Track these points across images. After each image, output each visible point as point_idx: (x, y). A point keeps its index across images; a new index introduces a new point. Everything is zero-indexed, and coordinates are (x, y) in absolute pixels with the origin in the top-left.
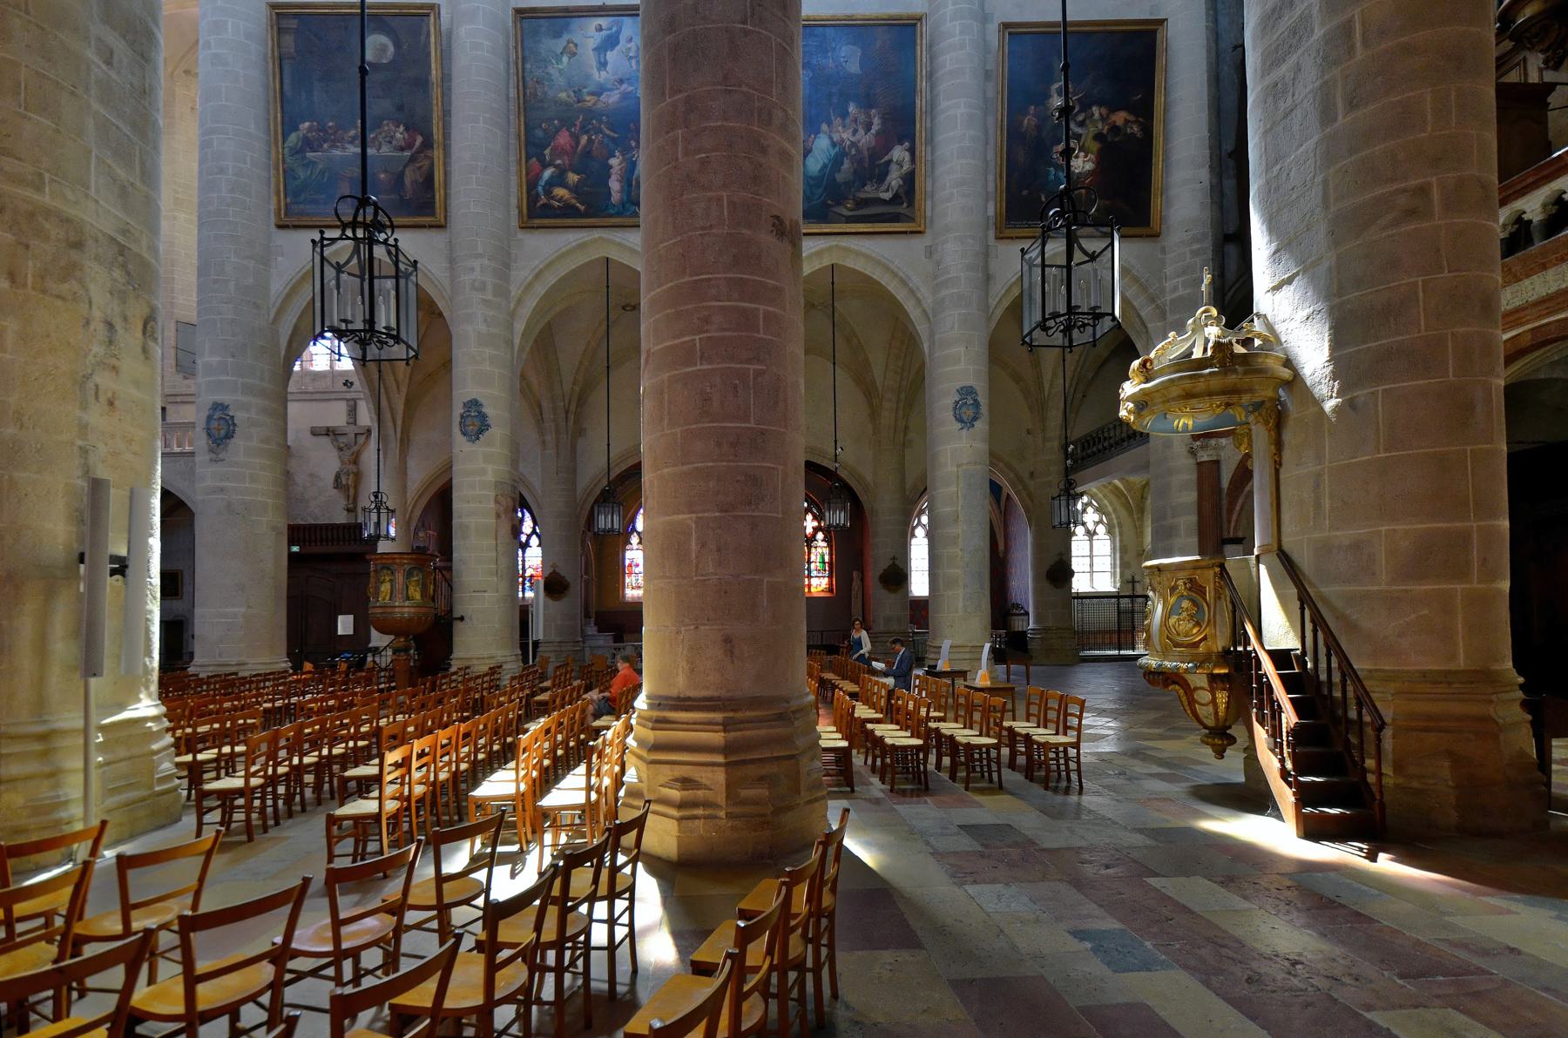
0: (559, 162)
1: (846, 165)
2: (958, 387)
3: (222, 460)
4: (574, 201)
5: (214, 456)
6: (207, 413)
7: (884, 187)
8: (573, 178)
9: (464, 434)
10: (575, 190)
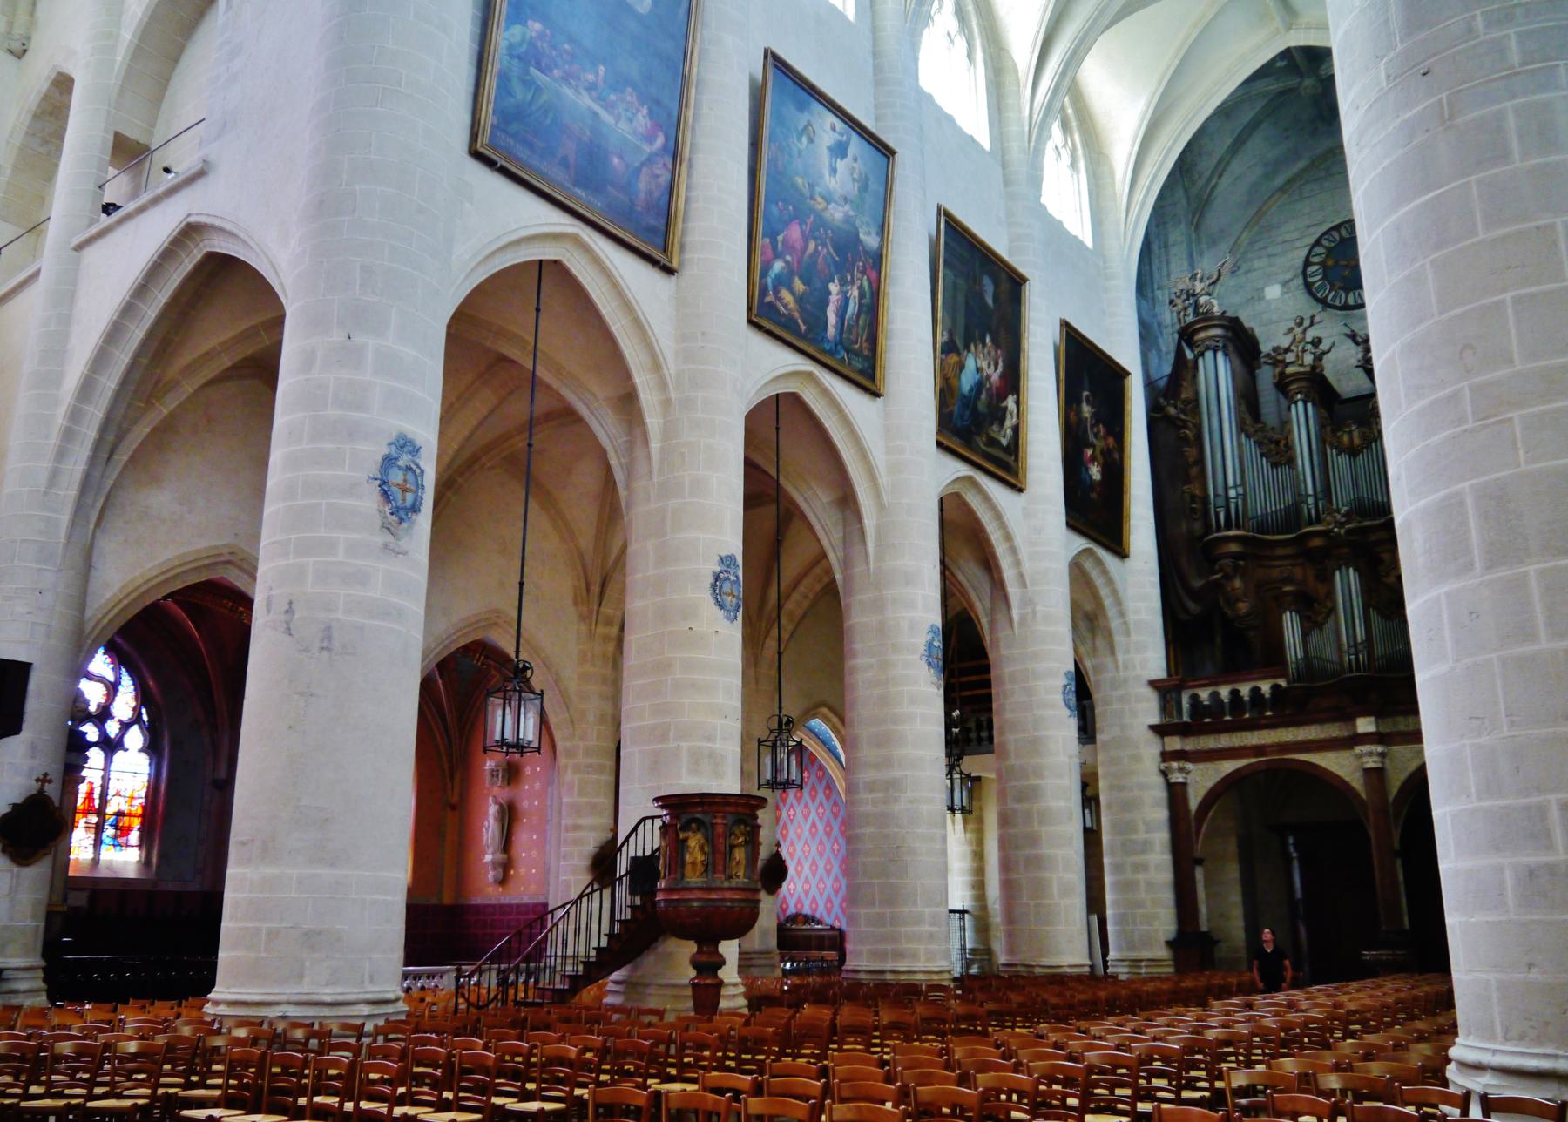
0: (788, 258)
1: (983, 396)
2: (1065, 670)
3: (405, 553)
4: (797, 315)
5: (390, 538)
6: (385, 450)
7: (1003, 433)
8: (799, 286)
9: (721, 605)
10: (800, 300)
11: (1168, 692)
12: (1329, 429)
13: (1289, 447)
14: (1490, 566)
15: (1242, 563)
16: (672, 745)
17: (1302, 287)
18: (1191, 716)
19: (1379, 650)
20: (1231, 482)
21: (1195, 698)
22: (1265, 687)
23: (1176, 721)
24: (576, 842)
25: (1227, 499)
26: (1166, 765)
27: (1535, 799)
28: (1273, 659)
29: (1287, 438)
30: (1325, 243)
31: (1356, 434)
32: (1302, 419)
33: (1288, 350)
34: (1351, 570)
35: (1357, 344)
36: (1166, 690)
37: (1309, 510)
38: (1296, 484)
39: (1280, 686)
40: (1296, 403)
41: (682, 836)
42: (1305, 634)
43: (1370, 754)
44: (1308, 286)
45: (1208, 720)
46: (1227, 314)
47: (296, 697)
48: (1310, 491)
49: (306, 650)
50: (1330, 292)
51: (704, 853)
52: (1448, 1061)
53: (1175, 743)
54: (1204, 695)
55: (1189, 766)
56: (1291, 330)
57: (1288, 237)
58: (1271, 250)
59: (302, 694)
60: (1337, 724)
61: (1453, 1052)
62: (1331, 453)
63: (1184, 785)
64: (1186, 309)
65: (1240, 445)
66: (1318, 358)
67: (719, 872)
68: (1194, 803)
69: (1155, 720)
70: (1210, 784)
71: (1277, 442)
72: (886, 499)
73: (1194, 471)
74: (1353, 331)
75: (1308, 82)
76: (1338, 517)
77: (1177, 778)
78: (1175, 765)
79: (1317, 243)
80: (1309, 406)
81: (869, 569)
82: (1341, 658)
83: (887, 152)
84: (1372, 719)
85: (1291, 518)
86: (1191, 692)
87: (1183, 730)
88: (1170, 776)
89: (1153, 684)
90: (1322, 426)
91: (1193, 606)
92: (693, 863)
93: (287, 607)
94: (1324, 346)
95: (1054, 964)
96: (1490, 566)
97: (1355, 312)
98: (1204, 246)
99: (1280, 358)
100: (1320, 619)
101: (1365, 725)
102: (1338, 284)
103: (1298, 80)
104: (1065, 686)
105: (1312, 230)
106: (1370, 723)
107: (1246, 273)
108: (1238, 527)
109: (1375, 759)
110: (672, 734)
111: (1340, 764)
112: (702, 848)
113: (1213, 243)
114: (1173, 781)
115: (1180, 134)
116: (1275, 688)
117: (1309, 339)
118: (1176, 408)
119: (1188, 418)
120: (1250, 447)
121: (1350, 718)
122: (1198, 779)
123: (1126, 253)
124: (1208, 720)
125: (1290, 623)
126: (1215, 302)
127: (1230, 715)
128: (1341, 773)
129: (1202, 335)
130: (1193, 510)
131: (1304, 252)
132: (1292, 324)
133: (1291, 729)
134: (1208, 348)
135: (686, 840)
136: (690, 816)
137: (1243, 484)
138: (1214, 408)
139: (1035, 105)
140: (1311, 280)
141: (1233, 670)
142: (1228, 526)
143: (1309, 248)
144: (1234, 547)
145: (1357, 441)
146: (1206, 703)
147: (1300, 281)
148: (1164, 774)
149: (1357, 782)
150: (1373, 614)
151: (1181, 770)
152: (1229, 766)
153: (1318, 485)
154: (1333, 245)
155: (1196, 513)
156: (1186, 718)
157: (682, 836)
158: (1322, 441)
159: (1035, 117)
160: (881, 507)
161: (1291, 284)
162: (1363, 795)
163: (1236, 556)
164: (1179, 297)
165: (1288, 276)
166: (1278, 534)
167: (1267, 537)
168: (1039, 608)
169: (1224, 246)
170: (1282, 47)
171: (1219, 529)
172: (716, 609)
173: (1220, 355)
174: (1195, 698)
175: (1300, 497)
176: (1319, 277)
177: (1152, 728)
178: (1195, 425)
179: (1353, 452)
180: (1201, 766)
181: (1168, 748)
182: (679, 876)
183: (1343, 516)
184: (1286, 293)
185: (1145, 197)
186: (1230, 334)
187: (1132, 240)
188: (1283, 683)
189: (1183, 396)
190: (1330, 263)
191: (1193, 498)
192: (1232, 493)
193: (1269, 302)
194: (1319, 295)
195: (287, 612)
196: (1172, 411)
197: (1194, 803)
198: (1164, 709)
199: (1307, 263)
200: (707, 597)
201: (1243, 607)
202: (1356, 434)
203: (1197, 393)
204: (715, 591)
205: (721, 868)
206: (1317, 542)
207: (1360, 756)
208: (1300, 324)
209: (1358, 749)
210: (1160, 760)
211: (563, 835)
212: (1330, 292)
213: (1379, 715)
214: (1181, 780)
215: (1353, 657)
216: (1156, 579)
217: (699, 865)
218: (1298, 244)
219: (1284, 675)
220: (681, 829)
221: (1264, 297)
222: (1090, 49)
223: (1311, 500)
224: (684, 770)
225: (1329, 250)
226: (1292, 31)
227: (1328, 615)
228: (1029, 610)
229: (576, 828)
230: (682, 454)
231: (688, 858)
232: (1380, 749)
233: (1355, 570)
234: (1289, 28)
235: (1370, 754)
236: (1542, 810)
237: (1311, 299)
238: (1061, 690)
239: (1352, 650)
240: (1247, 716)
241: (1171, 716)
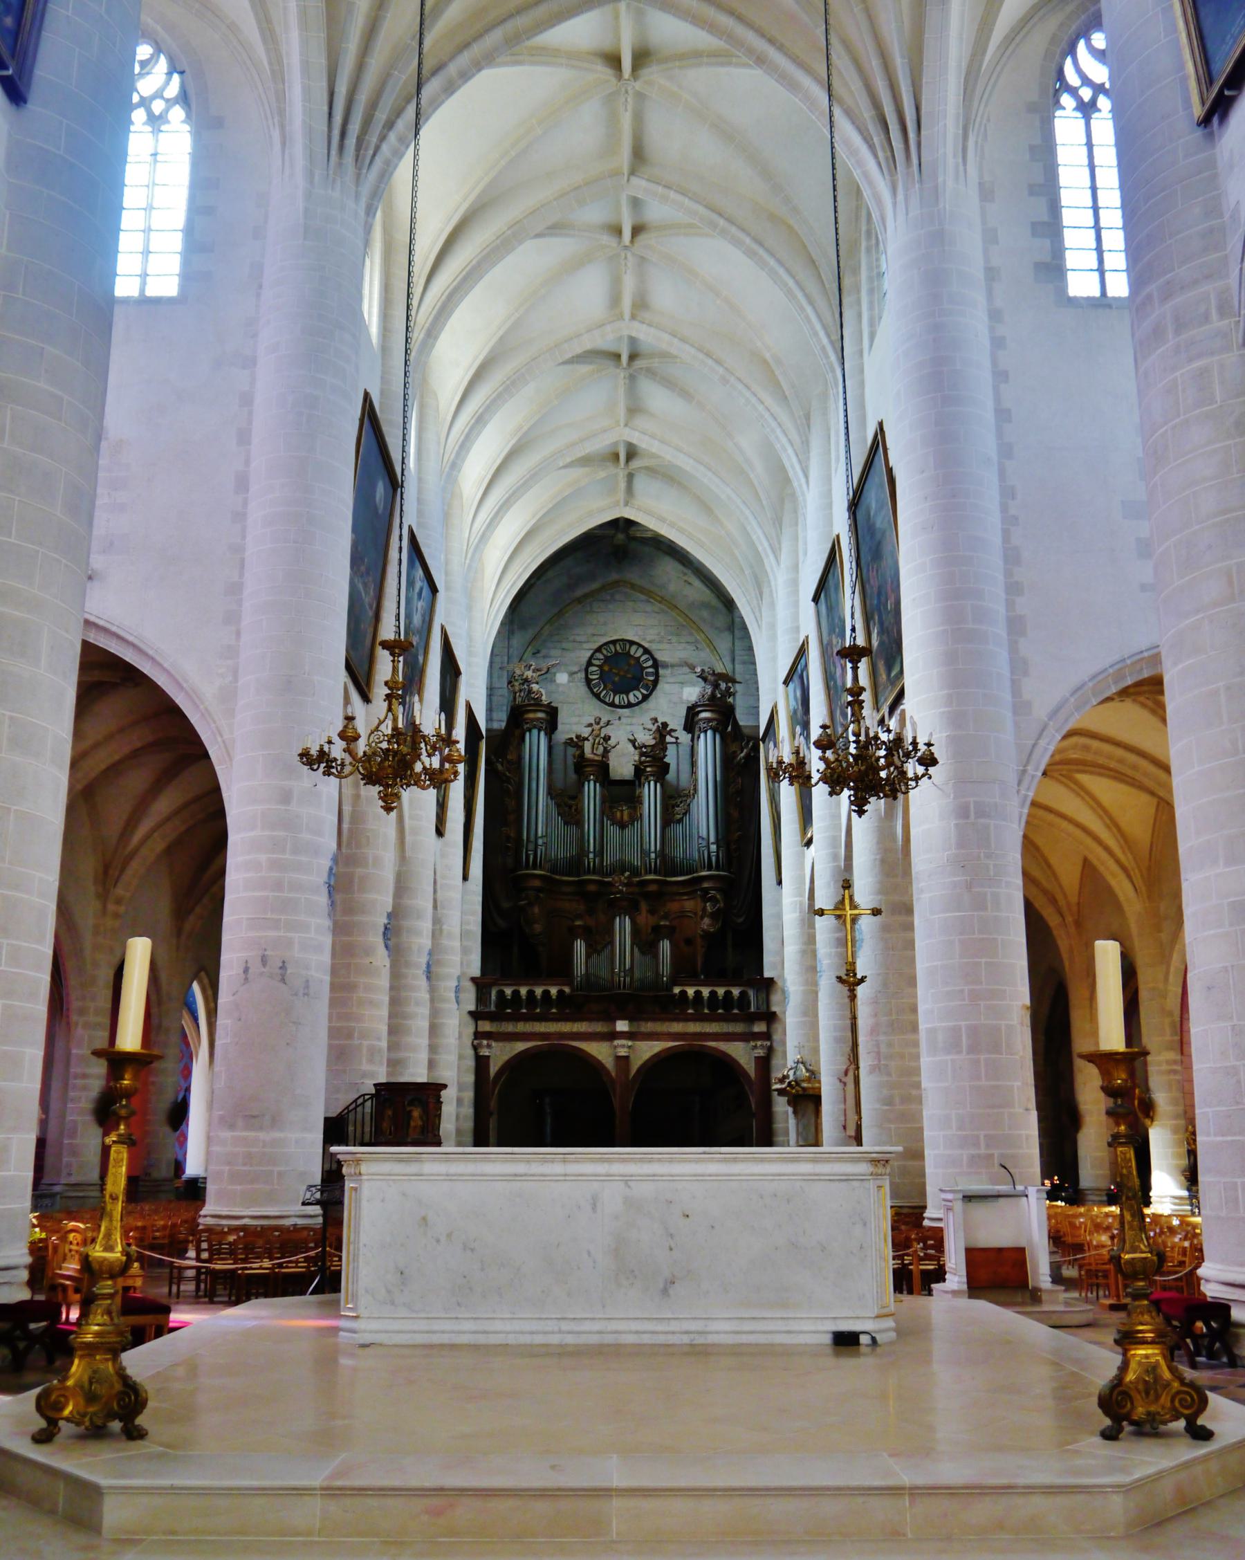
12: (607, 804)
13: (579, 811)
14: (968, 1053)
15: (541, 895)
16: (356, 1042)
17: (584, 680)
18: (496, 1006)
19: (637, 975)
20: (540, 834)
21: (501, 994)
22: (554, 991)
24: (85, 1088)
25: (536, 845)
27: (975, 1133)
28: (561, 968)
29: (577, 805)
30: (605, 652)
31: (626, 813)
32: (591, 792)
33: (587, 739)
34: (627, 917)
35: (635, 748)
36: (481, 985)
37: (589, 863)
38: (582, 839)
39: (564, 991)
40: (589, 782)
41: (408, 1109)
42: (588, 956)
43: (623, 1046)
44: (588, 681)
45: (509, 1011)
46: (552, 704)
47: (291, 1024)
48: (592, 849)
49: (296, 994)
50: (603, 690)
52: (924, 1219)
53: (486, 1026)
54: (508, 991)
55: (494, 1044)
56: (590, 725)
57: (578, 638)
58: (565, 645)
59: (294, 1023)
60: (601, 1023)
61: (925, 1215)
62: (607, 823)
63: (488, 1057)
64: (520, 691)
65: (547, 803)
66: (606, 751)
68: (493, 1069)
69: (472, 1008)
70: (506, 1058)
71: (570, 807)
72: (408, 854)
74: (635, 739)
75: (621, 537)
76: (623, 878)
77: (484, 1052)
78: (485, 1042)
79: (598, 650)
80: (598, 785)
82: (613, 977)
83: (434, 590)
84: (627, 1022)
85: (575, 864)
87: (491, 1017)
88: (479, 1050)
89: (473, 980)
90: (603, 801)
91: (501, 923)
92: (415, 1127)
93: (281, 965)
94: (612, 742)
96: (968, 1053)
97: (618, 710)
98: (516, 627)
99: (580, 744)
100: (599, 948)
101: (622, 1026)
102: (610, 686)
103: (613, 532)
104: (457, 987)
105: (595, 638)
106: (625, 1024)
107: (545, 657)
108: (541, 868)
109: (626, 1050)
110: (356, 1034)
111: (600, 1051)
112: (421, 1118)
113: (523, 627)
114: (481, 1054)
115: (537, 556)
116: (560, 992)
117: (602, 735)
118: (502, 765)
120: (552, 804)
121: (613, 1020)
122: (498, 1053)
123: (486, 636)
124: (509, 1011)
125: (580, 947)
126: (544, 693)
127: (526, 1009)
128: (600, 1058)
129: (531, 715)
131: (589, 654)
132: (593, 722)
133: (568, 1023)
134: (535, 727)
135: (410, 1112)
137: (546, 836)
138: (534, 775)
139: (472, 531)
140: (591, 677)
141: (532, 973)
142: (535, 867)
143: (592, 651)
144: (537, 883)
145: (626, 818)
146: (509, 997)
147: (582, 675)
148: (475, 1048)
149: (609, 1063)
150: (636, 950)
151: (489, 1046)
152: (521, 1046)
153: (597, 846)
154: (609, 655)
156: (493, 1008)
158: (603, 813)
159: (471, 540)
161: (575, 675)
162: (613, 1074)
163: (539, 890)
164: (517, 680)
165: (575, 669)
166: (566, 875)
167: (557, 877)
168: (445, 927)
169: (530, 633)
170: (618, 516)
171: (527, 867)
173: (542, 734)
174: (501, 994)
175: (583, 852)
176: (597, 677)
177: (470, 1013)
179: (623, 826)
180: (501, 1044)
181: (480, 1029)
183: (625, 878)
184: (572, 682)
185: (506, 596)
186: (549, 718)
187: (491, 627)
188: (567, 990)
189: (509, 757)
190: (606, 668)
192: (540, 842)
193: (558, 685)
194: (595, 690)
195: (281, 968)
196: (500, 767)
197: (493, 1069)
199: (589, 664)
201: (538, 928)
202: (626, 813)
203: (520, 758)
206: (592, 888)
207: (615, 1047)
208: (598, 723)
209: (616, 1042)
211: (72, 1081)
212: (603, 690)
213: (631, 1019)
214: (487, 1054)
215: (622, 979)
216: (480, 899)
218: (585, 646)
219: (570, 984)
221: (555, 681)
222: (518, 500)
223: (591, 856)
224: (364, 1061)
225: (607, 659)
226: (628, 508)
227: (605, 946)
228: (438, 927)
229: (84, 1076)
230: (368, 838)
231: (412, 1124)
232: (630, 1043)
233: (629, 918)
234: (626, 504)
235: (623, 1046)
236: (978, 1137)
237: (589, 693)
238: (454, 989)
239: (622, 974)
240: (538, 1010)
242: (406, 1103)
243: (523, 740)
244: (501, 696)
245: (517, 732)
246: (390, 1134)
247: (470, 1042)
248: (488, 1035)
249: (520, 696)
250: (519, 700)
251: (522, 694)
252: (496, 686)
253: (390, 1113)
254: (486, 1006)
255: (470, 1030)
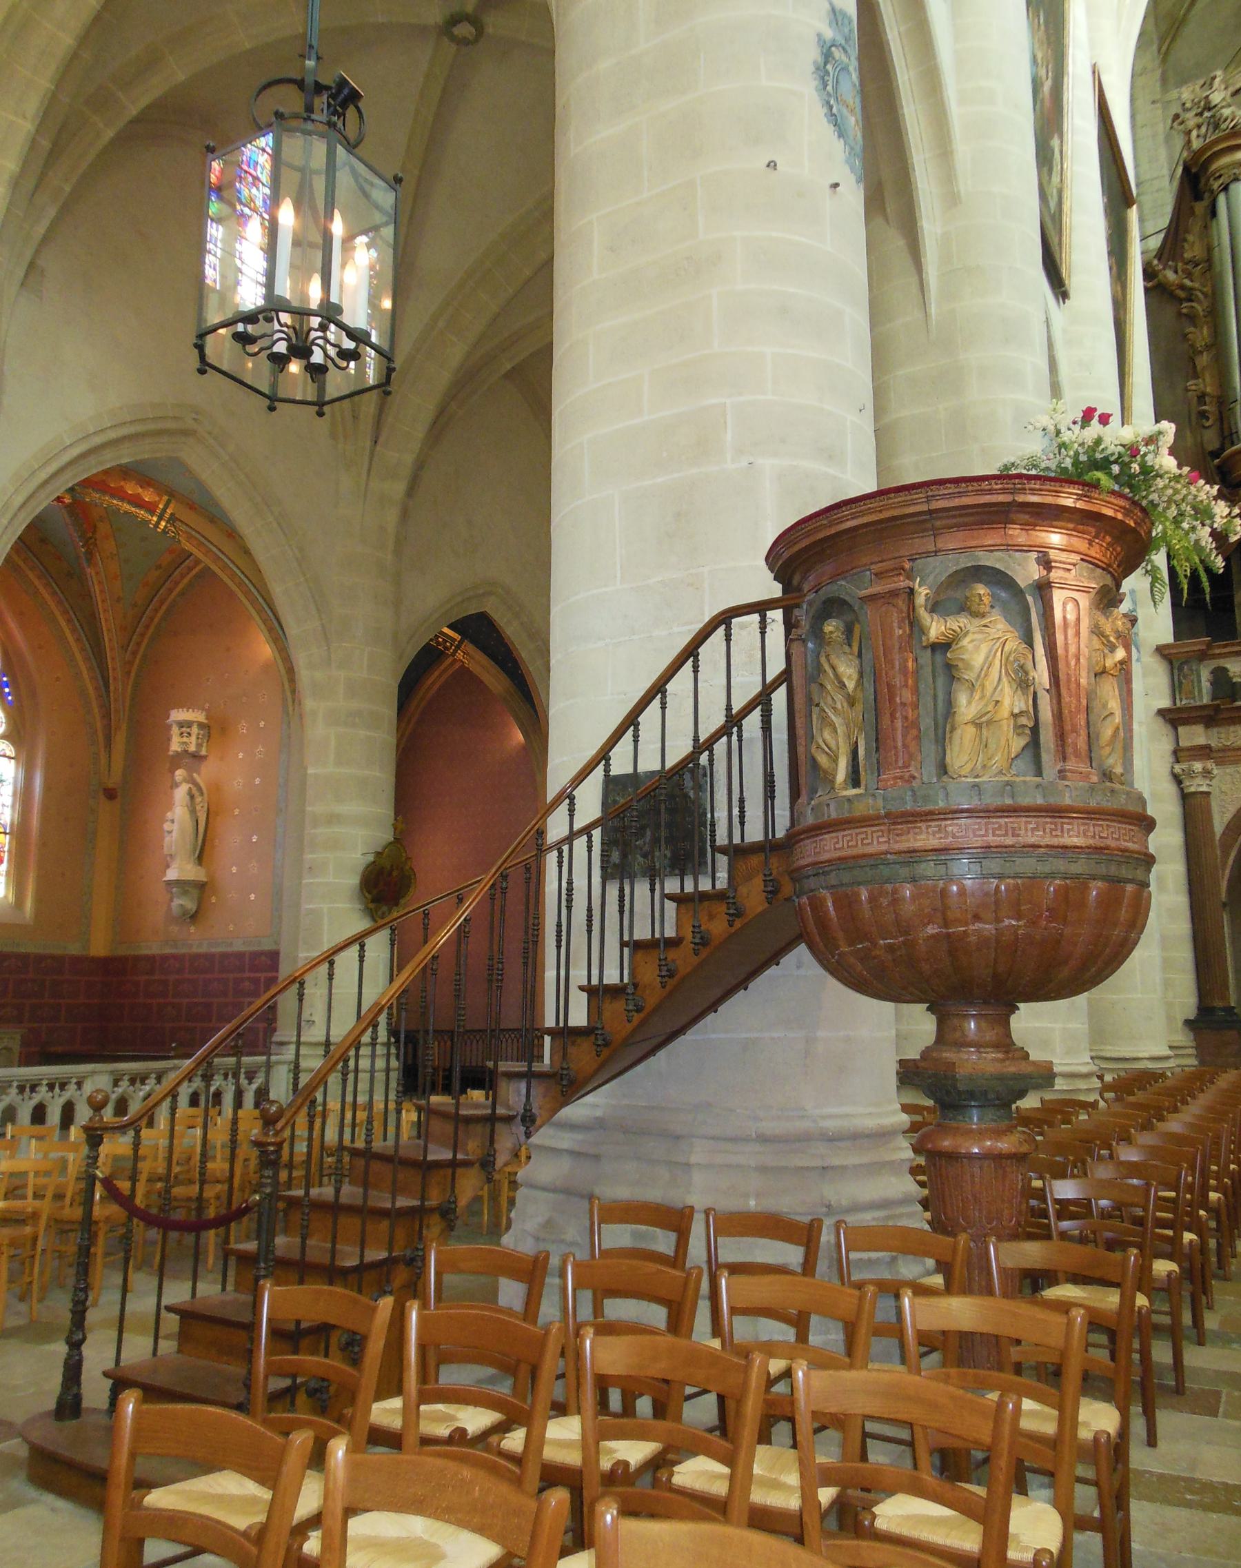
11: (1185, 663)
23: (1198, 703)
26: (1185, 766)
41: (936, 628)
51: (1023, 683)
53: (1196, 735)
63: (1208, 794)
64: (1199, 127)
67: (1077, 754)
68: (1219, 825)
69: (1165, 703)
73: (1203, 360)
77: (1196, 785)
78: (1198, 766)
81: (926, 315)
86: (1214, 664)
87: (1210, 717)
88: (1186, 783)
95: (1127, 1055)
114: (1192, 789)
118: (1176, 272)
119: (1196, 285)
130: (1203, 415)
136: (965, 562)
148: (1177, 779)
151: (1207, 773)
155: (1208, 419)
157: (936, 628)
160: (952, 199)
172: (829, 131)
177: (1161, 713)
178: (1205, 295)
180: (1230, 769)
182: (928, 773)
189: (1187, 255)
191: (1202, 398)
196: (1170, 276)
197: (1219, 825)
198: (1176, 688)
200: (808, 89)
203: (1209, 249)
204: (825, 85)
205: (1082, 742)
210: (1170, 759)
214: (1204, 789)
217: (1007, 727)
220: (935, 607)
231: (967, 707)
241: (1190, 695)
242: (920, 600)
243: (1213, 213)
244: (1157, 191)
245: (1200, 207)
246: (854, 779)
247: (1169, 766)
248: (1204, 752)
249: (1198, 136)
250: (1196, 144)
251: (1203, 129)
252: (1148, 177)
253: (848, 671)
254: (1194, 698)
255: (1166, 746)
